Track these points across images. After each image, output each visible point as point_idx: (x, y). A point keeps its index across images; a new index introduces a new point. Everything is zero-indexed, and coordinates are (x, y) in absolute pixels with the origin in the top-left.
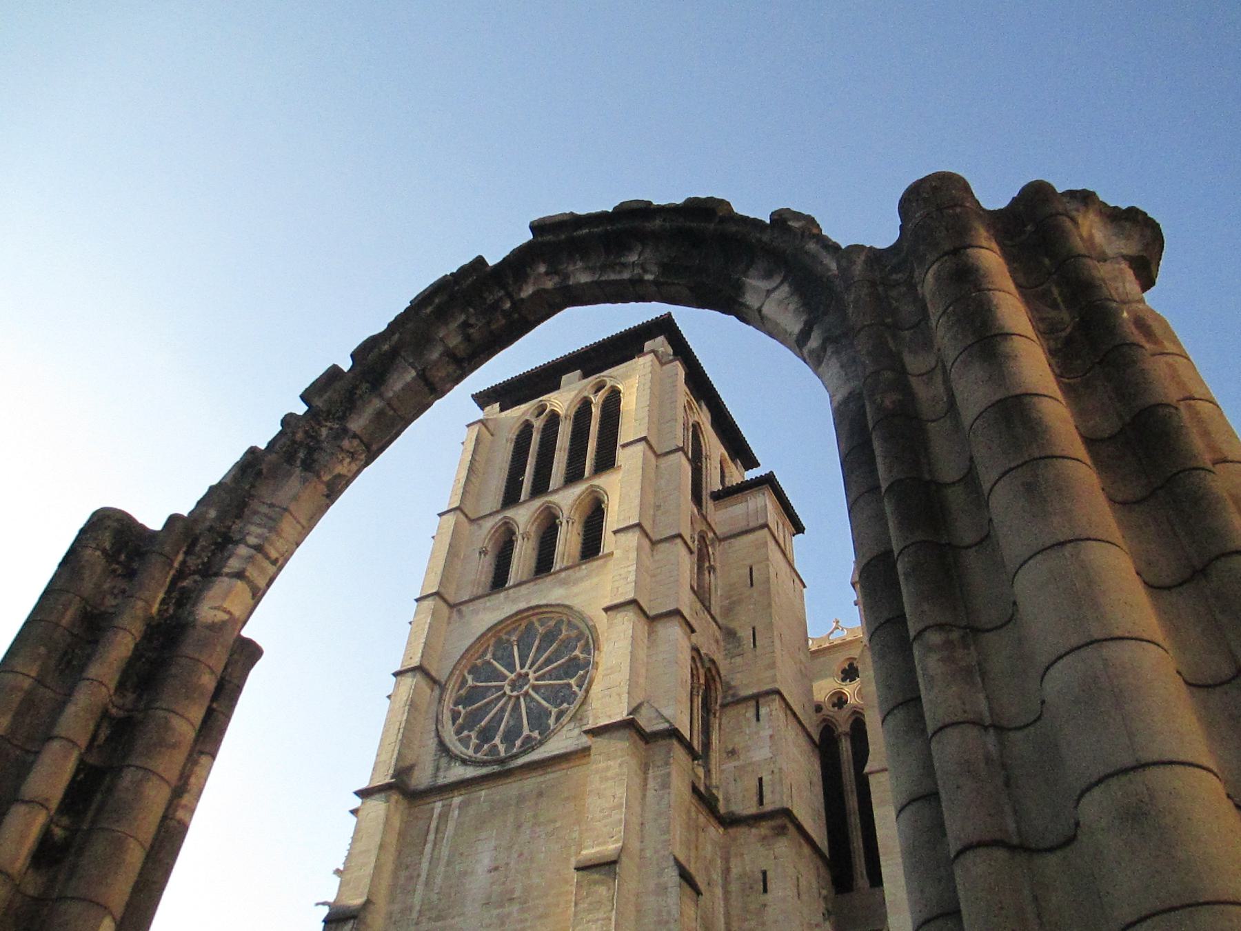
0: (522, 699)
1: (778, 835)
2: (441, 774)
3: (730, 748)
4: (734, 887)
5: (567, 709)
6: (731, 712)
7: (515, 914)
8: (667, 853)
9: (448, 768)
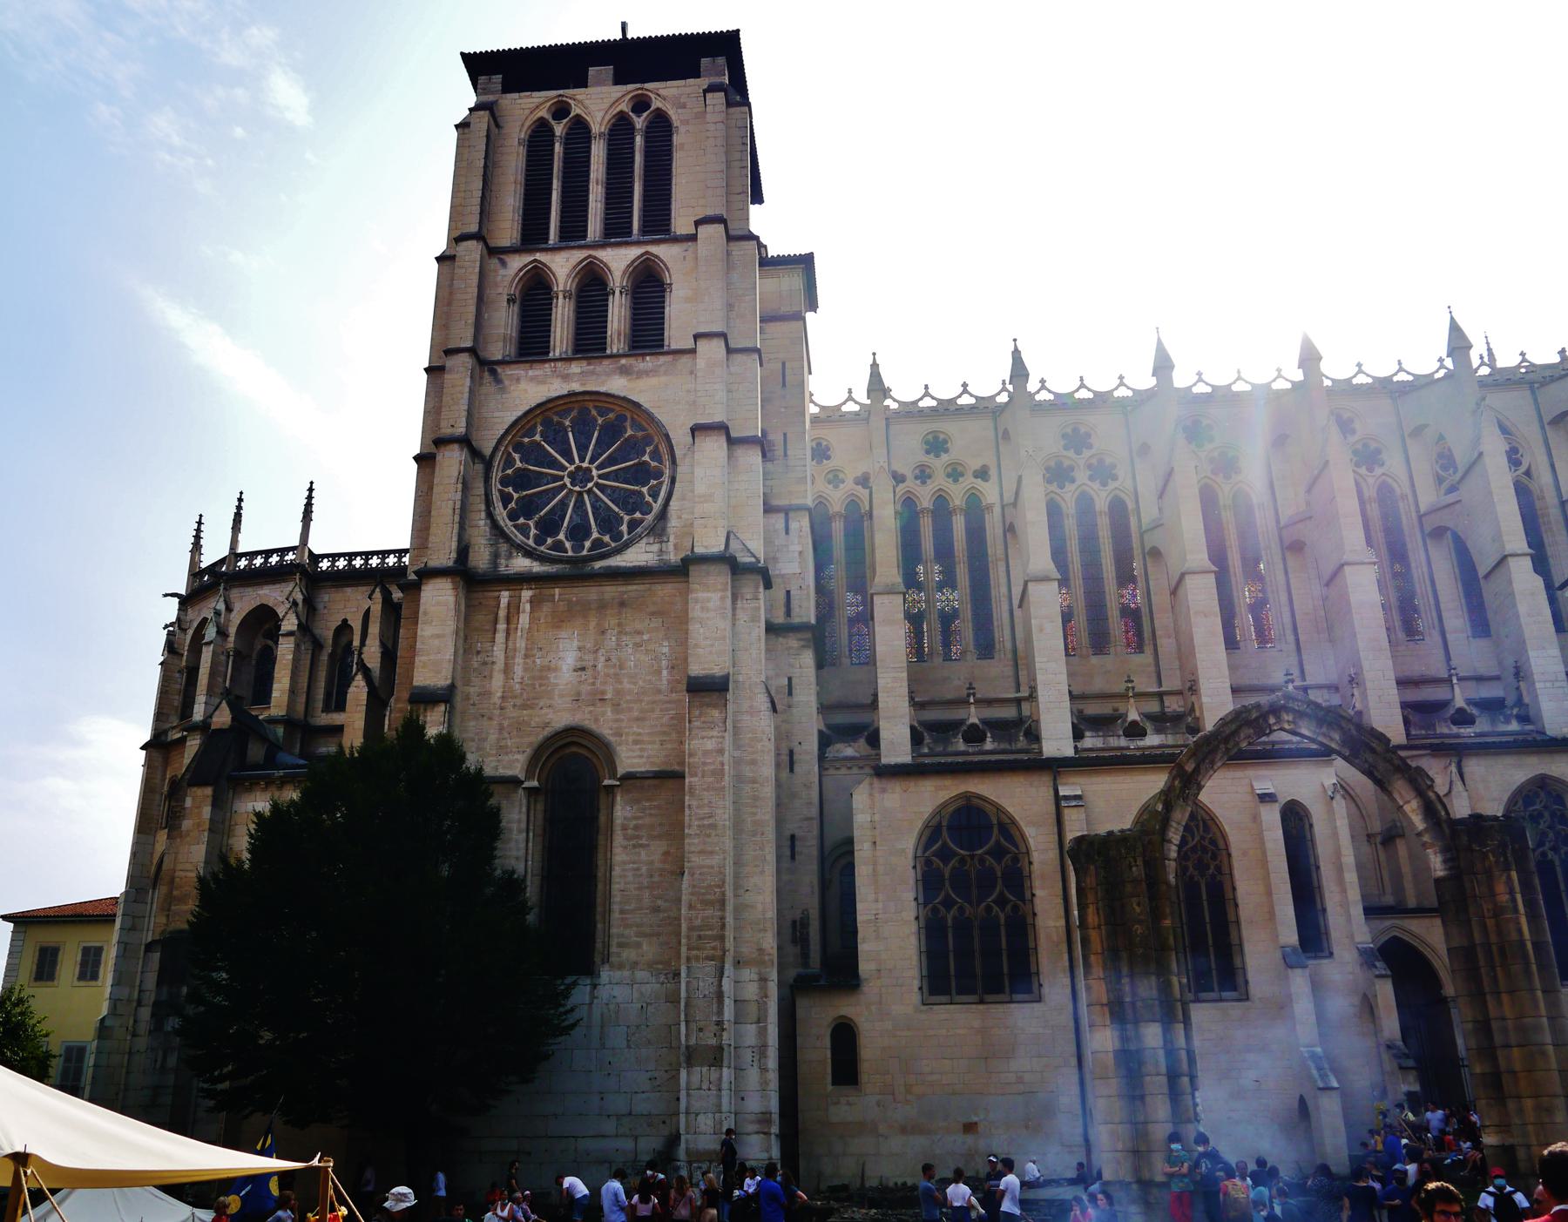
0: (586, 496)
1: (803, 646)
5: (642, 521)
7: (609, 714)
8: (758, 680)
9: (510, 556)
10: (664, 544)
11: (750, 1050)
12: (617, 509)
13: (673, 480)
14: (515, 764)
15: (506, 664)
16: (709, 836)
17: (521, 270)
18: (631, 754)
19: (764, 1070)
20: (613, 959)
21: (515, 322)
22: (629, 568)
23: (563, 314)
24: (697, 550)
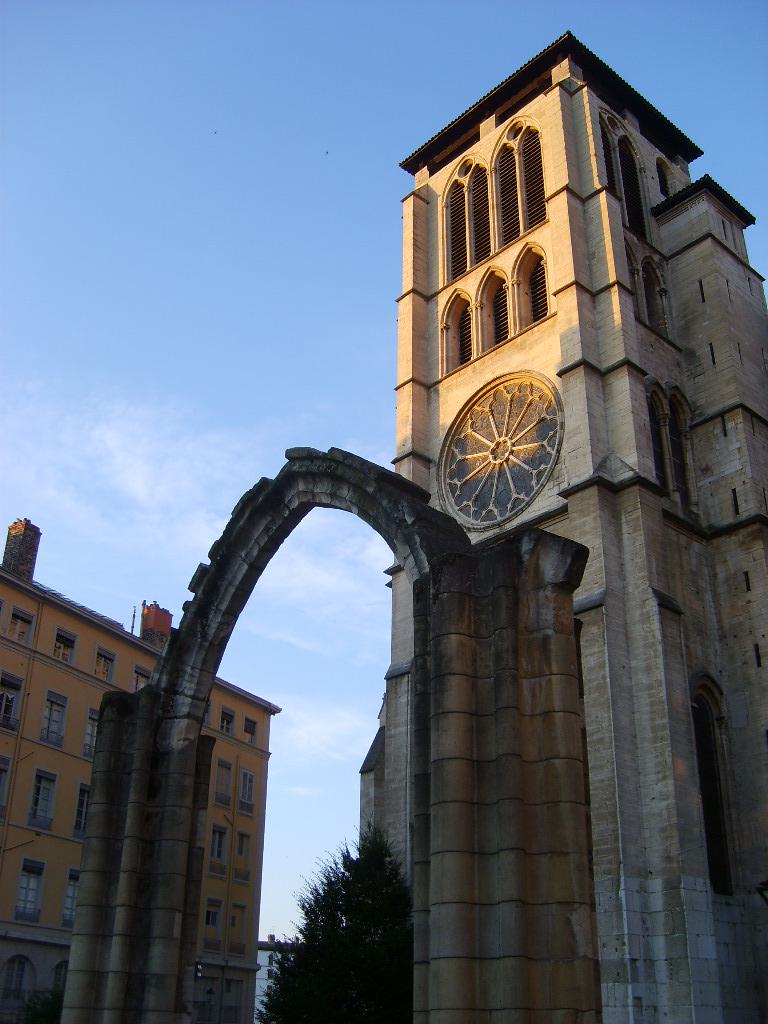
1: (755, 539)
3: (703, 466)
4: (722, 589)
6: (700, 430)
13: (562, 425)
17: (447, 303)
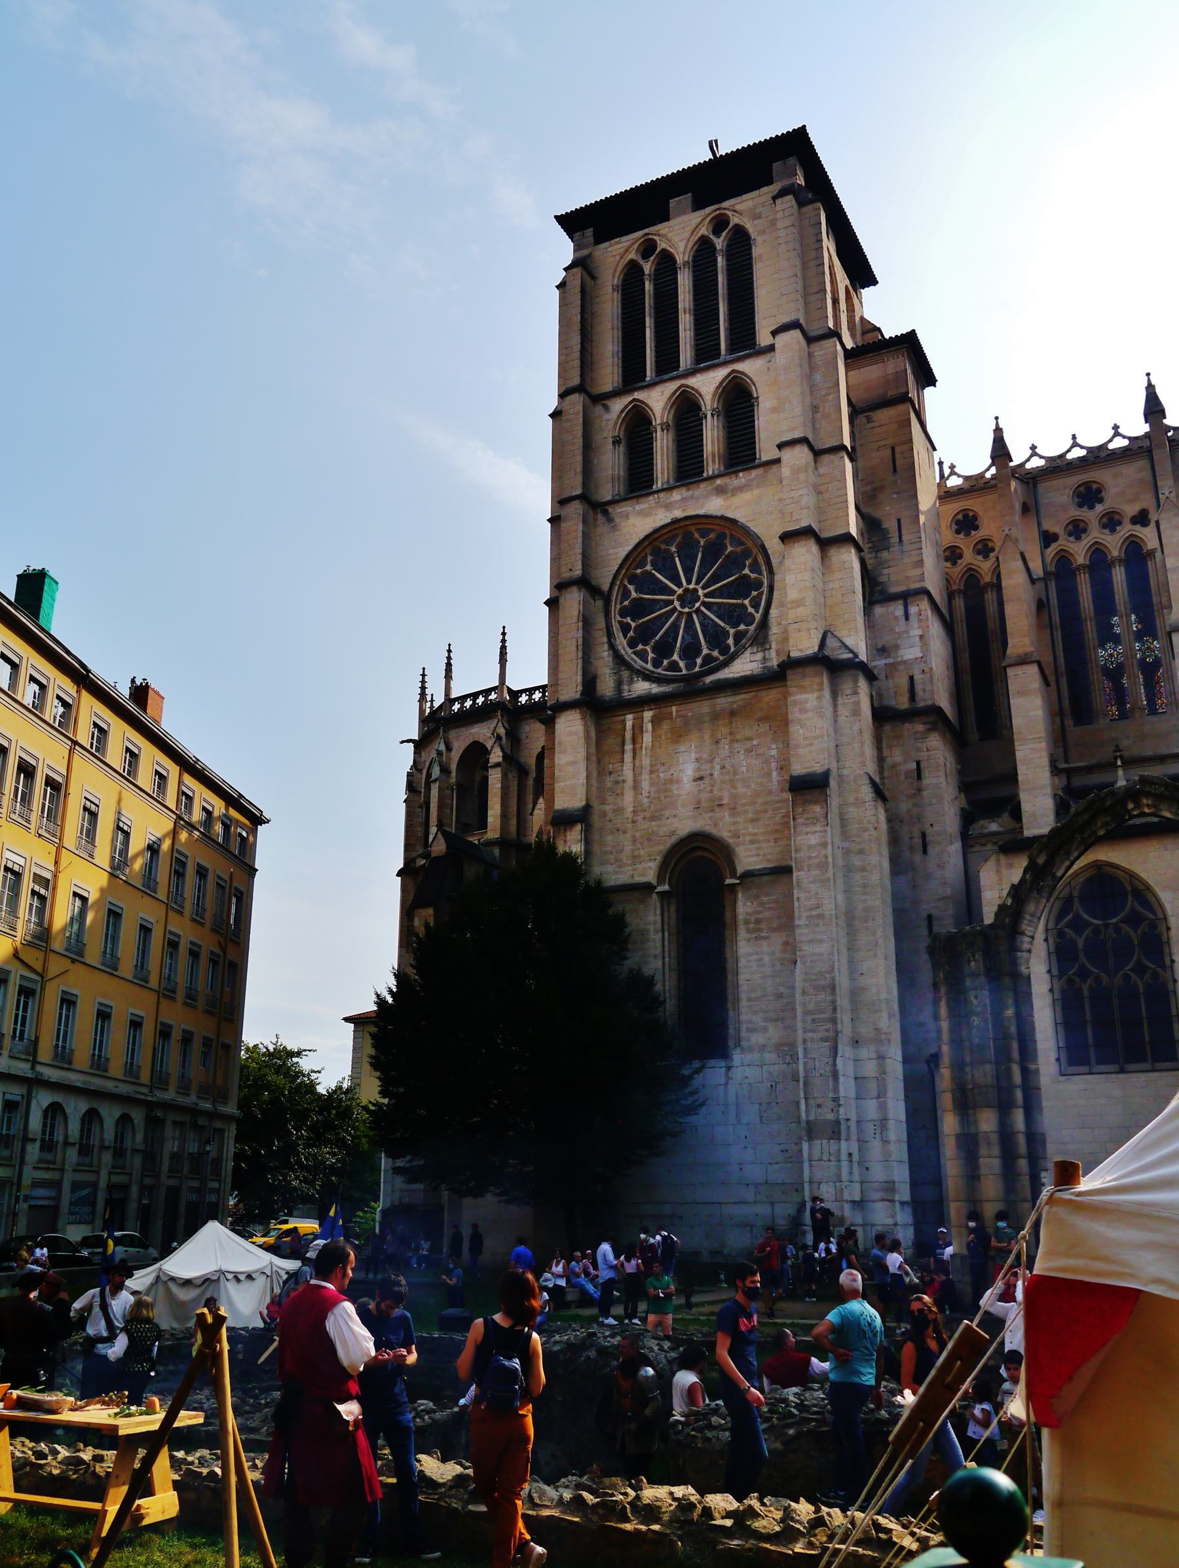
0: (695, 616)
1: (929, 730)
2: (626, 687)
3: (880, 645)
5: (746, 632)
7: (727, 817)
8: (862, 772)
9: (631, 682)
10: (767, 652)
11: (871, 1125)
12: (722, 624)
13: (771, 589)
14: (648, 872)
15: (634, 781)
16: (817, 925)
17: (622, 411)
18: (748, 853)
19: (886, 1142)
20: (744, 1043)
21: (622, 462)
22: (737, 678)
23: (662, 447)
24: (792, 655)
